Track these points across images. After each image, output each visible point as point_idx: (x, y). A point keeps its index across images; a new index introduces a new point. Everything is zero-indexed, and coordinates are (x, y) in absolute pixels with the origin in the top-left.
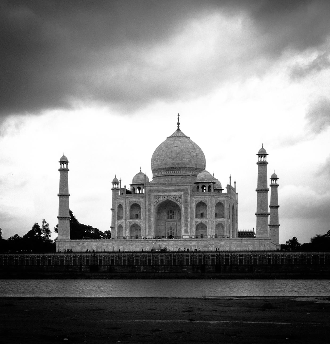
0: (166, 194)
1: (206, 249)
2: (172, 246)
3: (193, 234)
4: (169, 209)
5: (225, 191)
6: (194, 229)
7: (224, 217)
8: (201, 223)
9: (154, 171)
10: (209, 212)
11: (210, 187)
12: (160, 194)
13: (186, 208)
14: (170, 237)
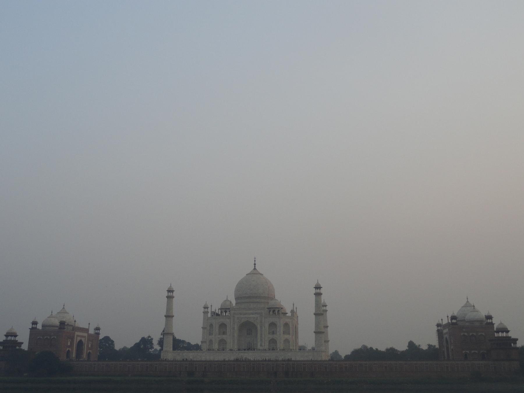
0: (247, 316)
2: (250, 356)
3: (266, 347)
4: (248, 328)
5: (289, 314)
7: (289, 334)
8: (273, 339)
9: (237, 299)
10: (278, 330)
11: (278, 311)
12: (242, 316)
14: (248, 349)
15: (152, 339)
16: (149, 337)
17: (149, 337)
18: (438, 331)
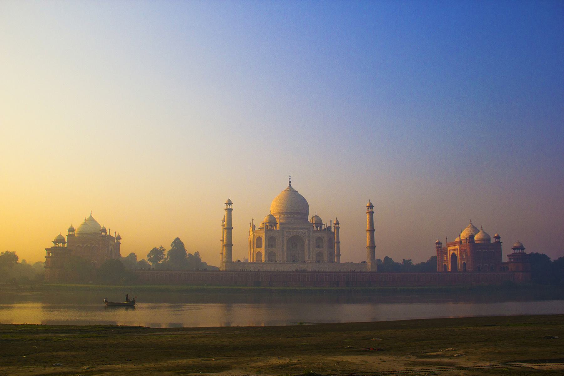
1: (334, 270)
6: (315, 256)
12: (291, 230)
13: (309, 241)
14: (294, 261)
15: (164, 250)
16: (161, 247)
17: (161, 247)
18: (437, 248)
